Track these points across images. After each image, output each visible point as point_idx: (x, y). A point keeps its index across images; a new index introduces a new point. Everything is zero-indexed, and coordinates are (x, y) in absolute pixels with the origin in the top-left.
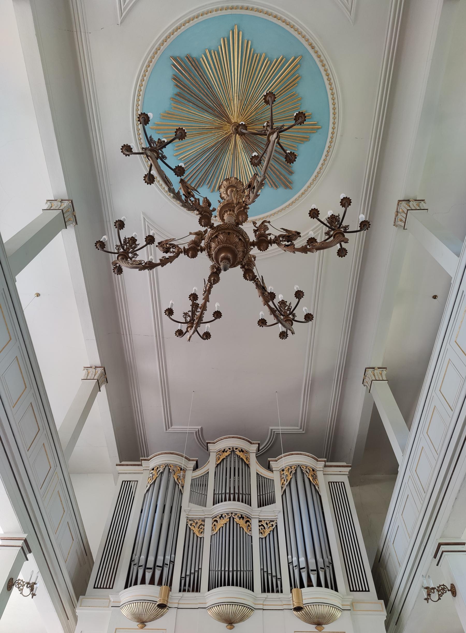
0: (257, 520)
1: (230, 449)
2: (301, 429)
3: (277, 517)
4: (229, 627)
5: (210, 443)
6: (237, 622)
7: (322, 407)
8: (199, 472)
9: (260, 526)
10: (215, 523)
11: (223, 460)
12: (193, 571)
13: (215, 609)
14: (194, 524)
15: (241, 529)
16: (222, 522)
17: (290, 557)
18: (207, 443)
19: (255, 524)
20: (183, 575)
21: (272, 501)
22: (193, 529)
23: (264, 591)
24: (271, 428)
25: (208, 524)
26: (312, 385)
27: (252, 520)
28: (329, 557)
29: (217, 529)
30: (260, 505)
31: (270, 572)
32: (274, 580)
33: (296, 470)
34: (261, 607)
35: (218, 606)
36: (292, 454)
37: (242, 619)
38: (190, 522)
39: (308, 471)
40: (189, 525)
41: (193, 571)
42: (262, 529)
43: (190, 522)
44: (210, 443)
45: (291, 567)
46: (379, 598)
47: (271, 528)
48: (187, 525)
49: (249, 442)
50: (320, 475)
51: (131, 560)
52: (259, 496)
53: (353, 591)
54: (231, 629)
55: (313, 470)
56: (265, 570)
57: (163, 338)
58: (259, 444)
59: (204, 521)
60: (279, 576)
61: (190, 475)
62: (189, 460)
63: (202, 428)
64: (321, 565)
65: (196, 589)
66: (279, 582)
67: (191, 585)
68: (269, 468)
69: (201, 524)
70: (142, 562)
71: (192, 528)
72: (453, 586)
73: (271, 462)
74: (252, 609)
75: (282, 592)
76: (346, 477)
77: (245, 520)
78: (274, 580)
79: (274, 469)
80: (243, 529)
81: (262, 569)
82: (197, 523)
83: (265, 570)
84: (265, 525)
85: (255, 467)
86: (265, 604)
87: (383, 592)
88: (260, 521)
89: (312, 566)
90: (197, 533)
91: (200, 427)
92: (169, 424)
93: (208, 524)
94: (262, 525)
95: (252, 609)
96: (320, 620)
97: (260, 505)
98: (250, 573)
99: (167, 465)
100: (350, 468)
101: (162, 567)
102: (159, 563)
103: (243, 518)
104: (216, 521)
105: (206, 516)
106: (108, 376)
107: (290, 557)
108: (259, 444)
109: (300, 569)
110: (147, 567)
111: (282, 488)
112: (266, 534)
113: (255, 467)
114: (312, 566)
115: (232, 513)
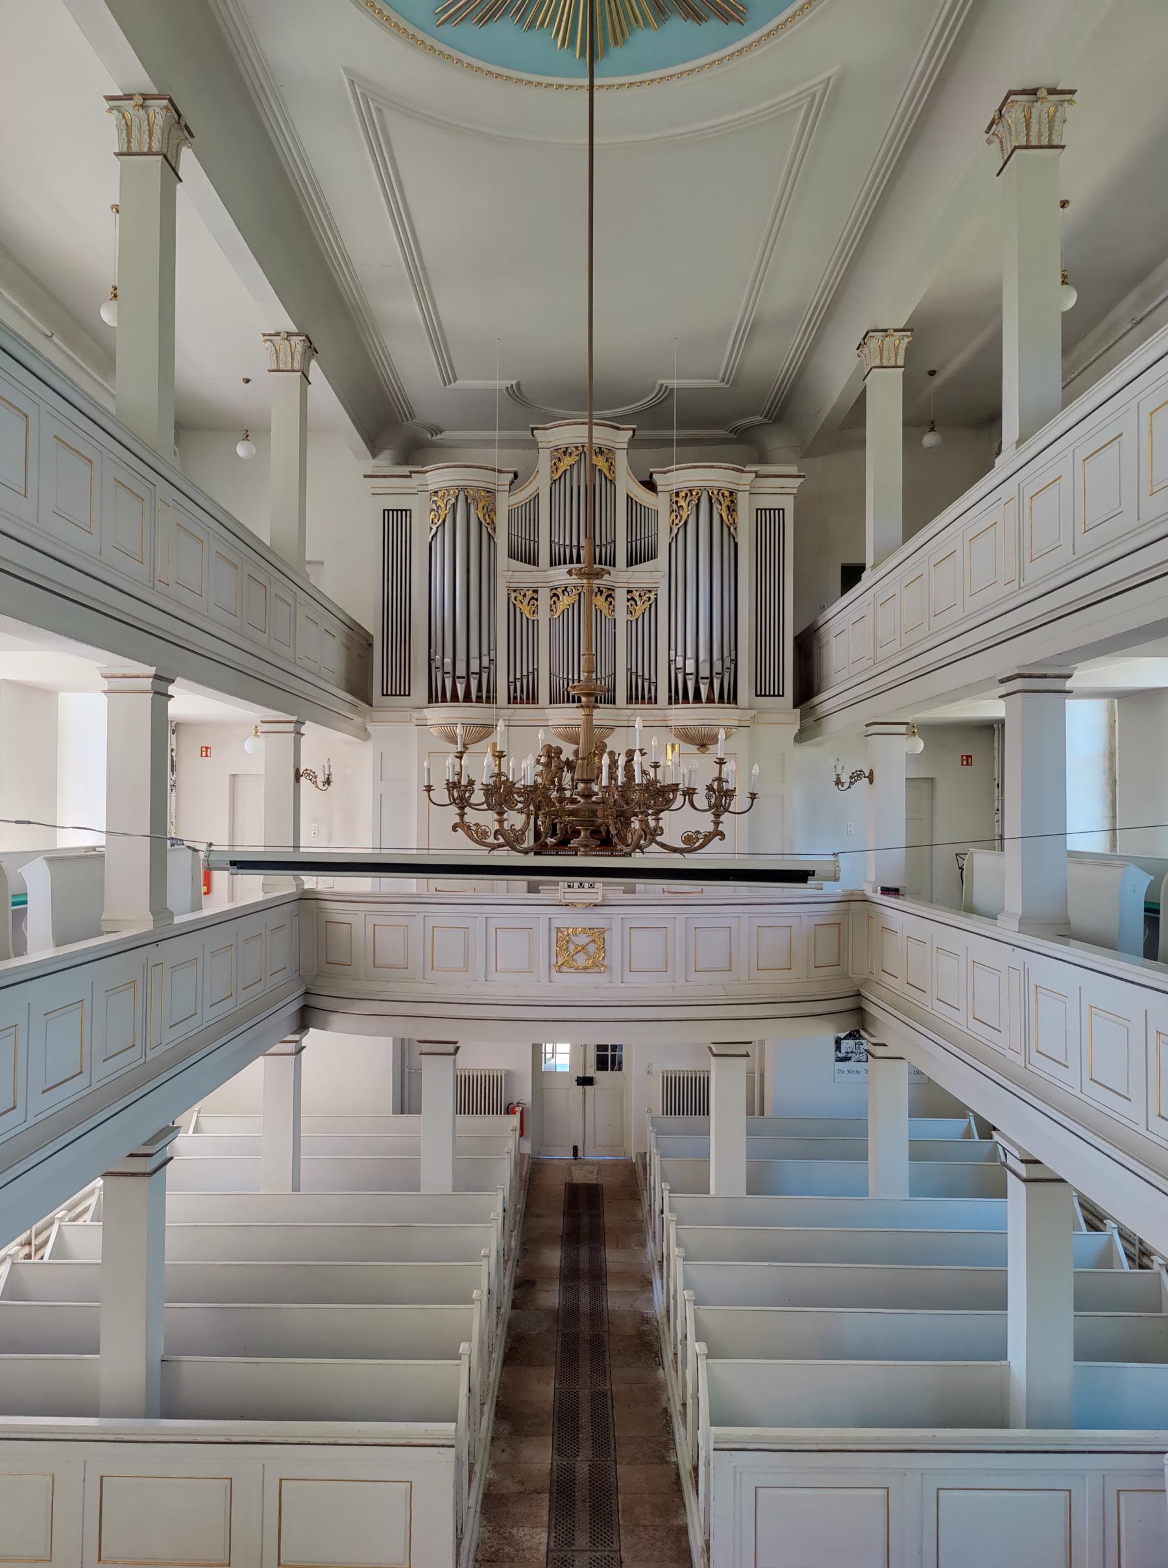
1: (577, 448)
2: (723, 381)
5: (537, 429)
7: (772, 357)
8: (522, 496)
9: (628, 600)
10: (555, 599)
11: (565, 471)
12: (525, 673)
14: (520, 598)
16: (565, 601)
17: (673, 653)
18: (533, 429)
19: (621, 597)
20: (512, 679)
21: (653, 555)
23: (630, 700)
24: (661, 382)
25: (544, 597)
26: (752, 330)
27: (617, 590)
28: (733, 653)
29: (559, 612)
30: (631, 562)
31: (640, 673)
32: (646, 685)
33: (699, 499)
36: (696, 467)
38: (513, 595)
39: (721, 499)
40: (512, 598)
41: (525, 673)
44: (537, 429)
45: (673, 667)
46: (796, 705)
47: (647, 604)
49: (614, 427)
50: (743, 500)
51: (430, 659)
52: (629, 542)
53: (761, 695)
55: (731, 493)
56: (634, 670)
57: (424, 269)
58: (634, 430)
59: (536, 591)
60: (653, 680)
61: (504, 503)
62: (500, 472)
63: (518, 384)
64: (717, 667)
65: (533, 698)
66: (653, 688)
67: (524, 695)
68: (650, 485)
69: (532, 598)
70: (448, 668)
71: (518, 603)
72: (871, 773)
73: (655, 476)
74: (611, 728)
75: (656, 703)
76: (792, 497)
77: (604, 595)
78: (646, 685)
79: (659, 489)
81: (629, 670)
82: (525, 596)
83: (634, 670)
84: (637, 599)
85: (626, 484)
87: (807, 689)
88: (629, 592)
89: (704, 671)
90: (527, 614)
91: (514, 382)
92: (450, 376)
93: (544, 597)
94: (633, 599)
95: (611, 728)
96: (705, 741)
97: (631, 562)
98: (611, 679)
99: (463, 489)
100: (802, 480)
101: (480, 674)
102: (475, 667)
103: (601, 592)
104: (555, 595)
106: (316, 344)
107: (673, 653)
108: (634, 430)
109: (686, 674)
110: (457, 674)
111: (671, 529)
112: (639, 613)
113: (626, 484)
114: (704, 671)
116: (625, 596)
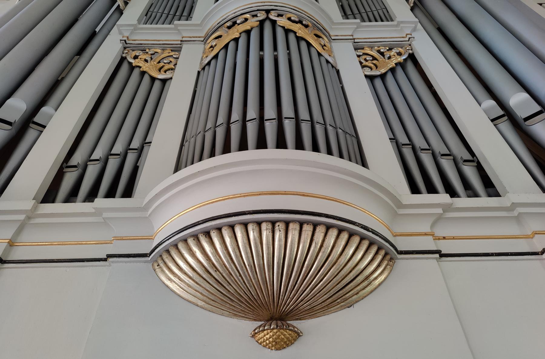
0: (350, 46)
3: (410, 36)
4: (267, 335)
6: (312, 312)
9: (359, 56)
13: (192, 258)
15: (303, 45)
22: (141, 64)
34: (428, 244)
35: (207, 234)
37: (341, 294)
42: (365, 60)
43: (134, 53)
48: (123, 59)
54: (280, 345)
74: (387, 252)
80: (309, 45)
86: (439, 232)
105: (184, 39)
115: (268, 12)
116: (354, 53)
